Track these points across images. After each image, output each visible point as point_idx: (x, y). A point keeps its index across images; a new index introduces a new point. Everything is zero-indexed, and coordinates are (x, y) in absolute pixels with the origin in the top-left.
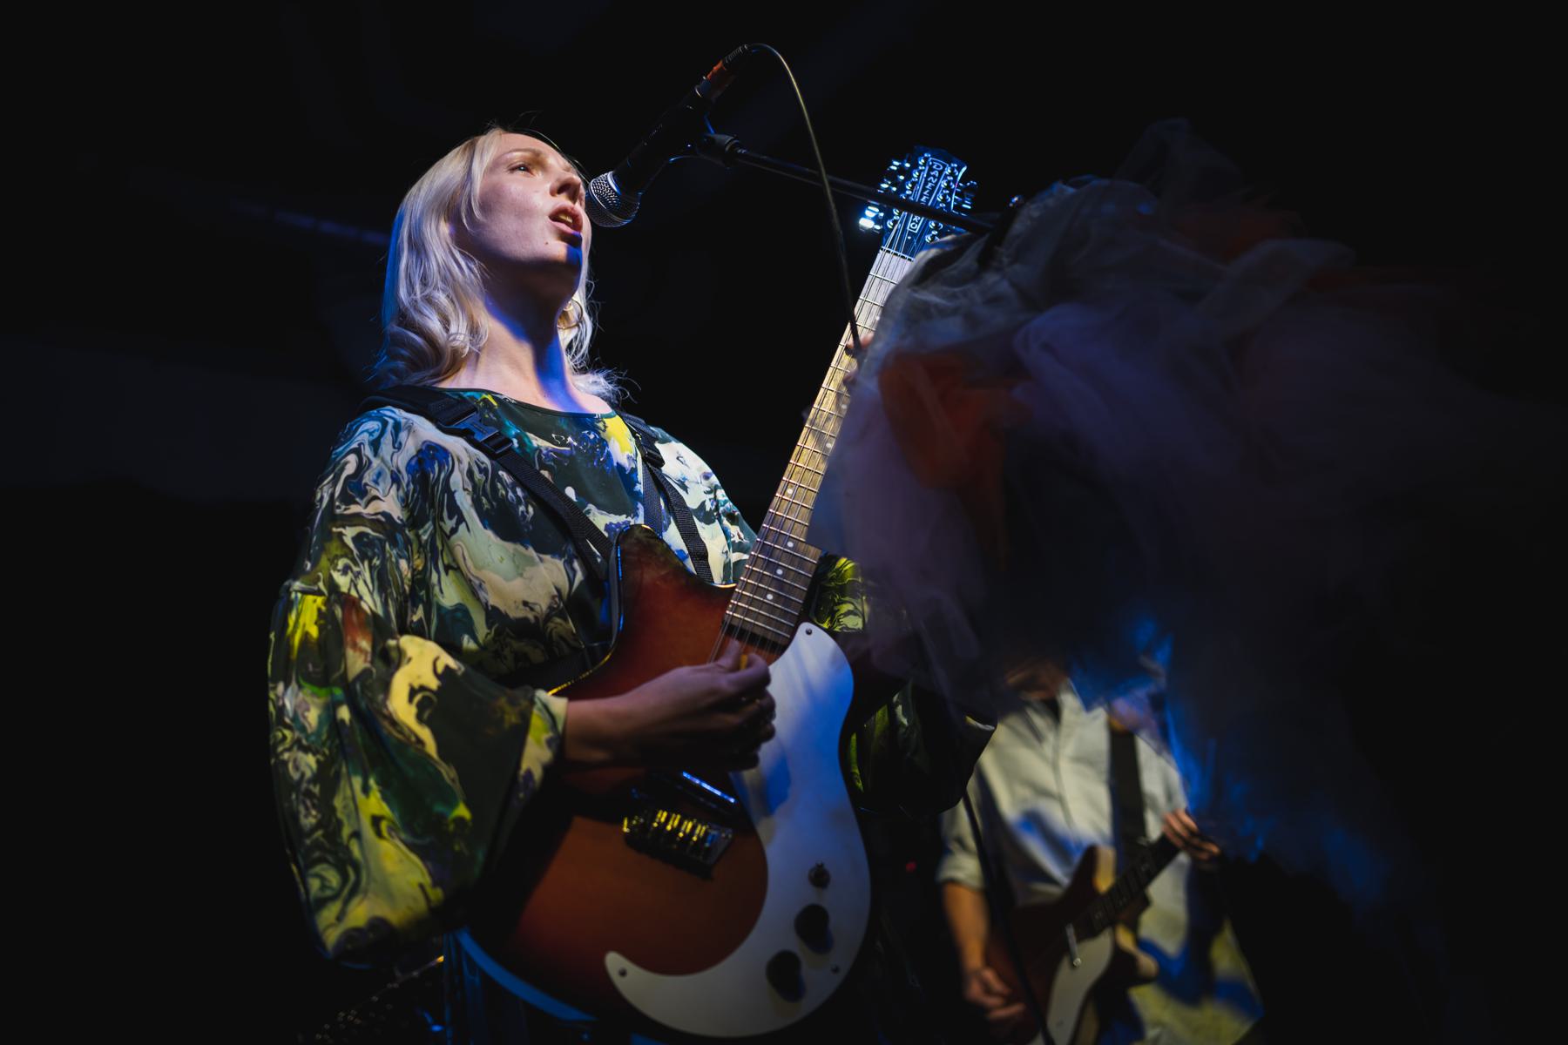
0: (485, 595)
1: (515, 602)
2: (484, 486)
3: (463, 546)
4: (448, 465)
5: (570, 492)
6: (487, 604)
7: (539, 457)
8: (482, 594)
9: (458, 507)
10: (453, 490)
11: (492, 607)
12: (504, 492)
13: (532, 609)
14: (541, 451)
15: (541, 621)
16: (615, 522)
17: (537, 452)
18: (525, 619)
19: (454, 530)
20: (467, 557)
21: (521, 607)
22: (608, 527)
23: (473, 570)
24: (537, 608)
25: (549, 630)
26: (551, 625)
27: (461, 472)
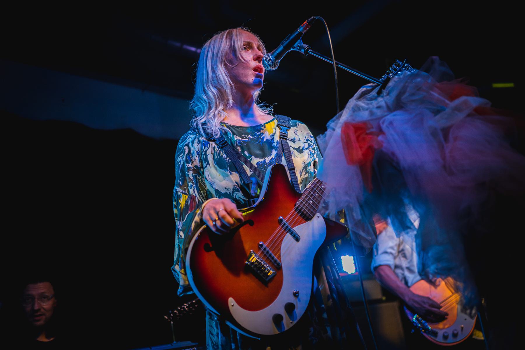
0: (214, 186)
1: (223, 188)
2: (217, 152)
3: (208, 171)
4: (208, 147)
5: (246, 153)
6: (215, 189)
7: (236, 143)
8: (213, 186)
9: (208, 160)
10: (207, 154)
11: (217, 189)
12: (222, 155)
13: (228, 190)
14: (237, 141)
15: (231, 193)
16: (261, 161)
17: (236, 141)
18: (226, 193)
19: (206, 167)
20: (209, 175)
21: (225, 189)
22: (257, 164)
23: (211, 179)
24: (229, 189)
25: (234, 196)
26: (234, 194)
27: (212, 148)
